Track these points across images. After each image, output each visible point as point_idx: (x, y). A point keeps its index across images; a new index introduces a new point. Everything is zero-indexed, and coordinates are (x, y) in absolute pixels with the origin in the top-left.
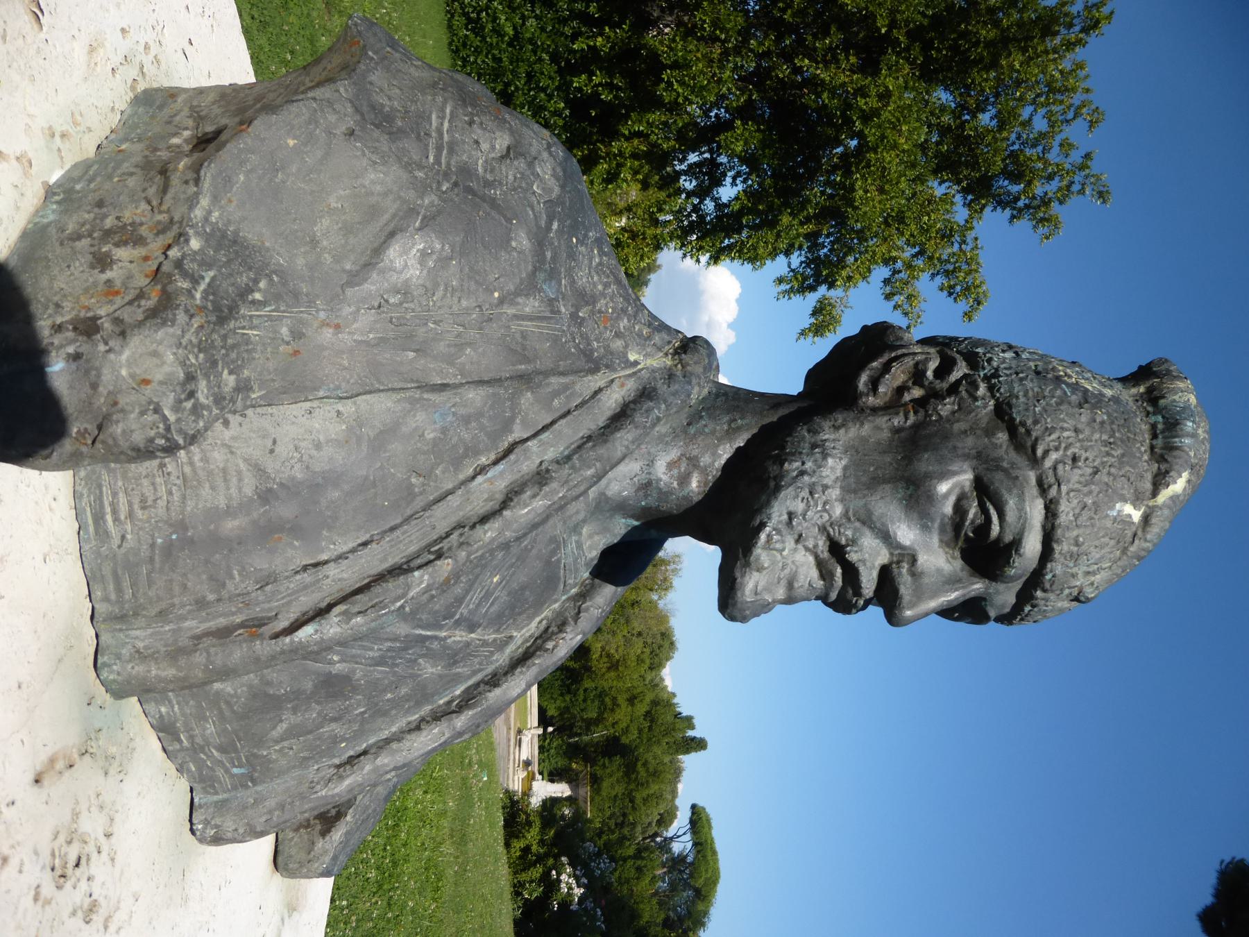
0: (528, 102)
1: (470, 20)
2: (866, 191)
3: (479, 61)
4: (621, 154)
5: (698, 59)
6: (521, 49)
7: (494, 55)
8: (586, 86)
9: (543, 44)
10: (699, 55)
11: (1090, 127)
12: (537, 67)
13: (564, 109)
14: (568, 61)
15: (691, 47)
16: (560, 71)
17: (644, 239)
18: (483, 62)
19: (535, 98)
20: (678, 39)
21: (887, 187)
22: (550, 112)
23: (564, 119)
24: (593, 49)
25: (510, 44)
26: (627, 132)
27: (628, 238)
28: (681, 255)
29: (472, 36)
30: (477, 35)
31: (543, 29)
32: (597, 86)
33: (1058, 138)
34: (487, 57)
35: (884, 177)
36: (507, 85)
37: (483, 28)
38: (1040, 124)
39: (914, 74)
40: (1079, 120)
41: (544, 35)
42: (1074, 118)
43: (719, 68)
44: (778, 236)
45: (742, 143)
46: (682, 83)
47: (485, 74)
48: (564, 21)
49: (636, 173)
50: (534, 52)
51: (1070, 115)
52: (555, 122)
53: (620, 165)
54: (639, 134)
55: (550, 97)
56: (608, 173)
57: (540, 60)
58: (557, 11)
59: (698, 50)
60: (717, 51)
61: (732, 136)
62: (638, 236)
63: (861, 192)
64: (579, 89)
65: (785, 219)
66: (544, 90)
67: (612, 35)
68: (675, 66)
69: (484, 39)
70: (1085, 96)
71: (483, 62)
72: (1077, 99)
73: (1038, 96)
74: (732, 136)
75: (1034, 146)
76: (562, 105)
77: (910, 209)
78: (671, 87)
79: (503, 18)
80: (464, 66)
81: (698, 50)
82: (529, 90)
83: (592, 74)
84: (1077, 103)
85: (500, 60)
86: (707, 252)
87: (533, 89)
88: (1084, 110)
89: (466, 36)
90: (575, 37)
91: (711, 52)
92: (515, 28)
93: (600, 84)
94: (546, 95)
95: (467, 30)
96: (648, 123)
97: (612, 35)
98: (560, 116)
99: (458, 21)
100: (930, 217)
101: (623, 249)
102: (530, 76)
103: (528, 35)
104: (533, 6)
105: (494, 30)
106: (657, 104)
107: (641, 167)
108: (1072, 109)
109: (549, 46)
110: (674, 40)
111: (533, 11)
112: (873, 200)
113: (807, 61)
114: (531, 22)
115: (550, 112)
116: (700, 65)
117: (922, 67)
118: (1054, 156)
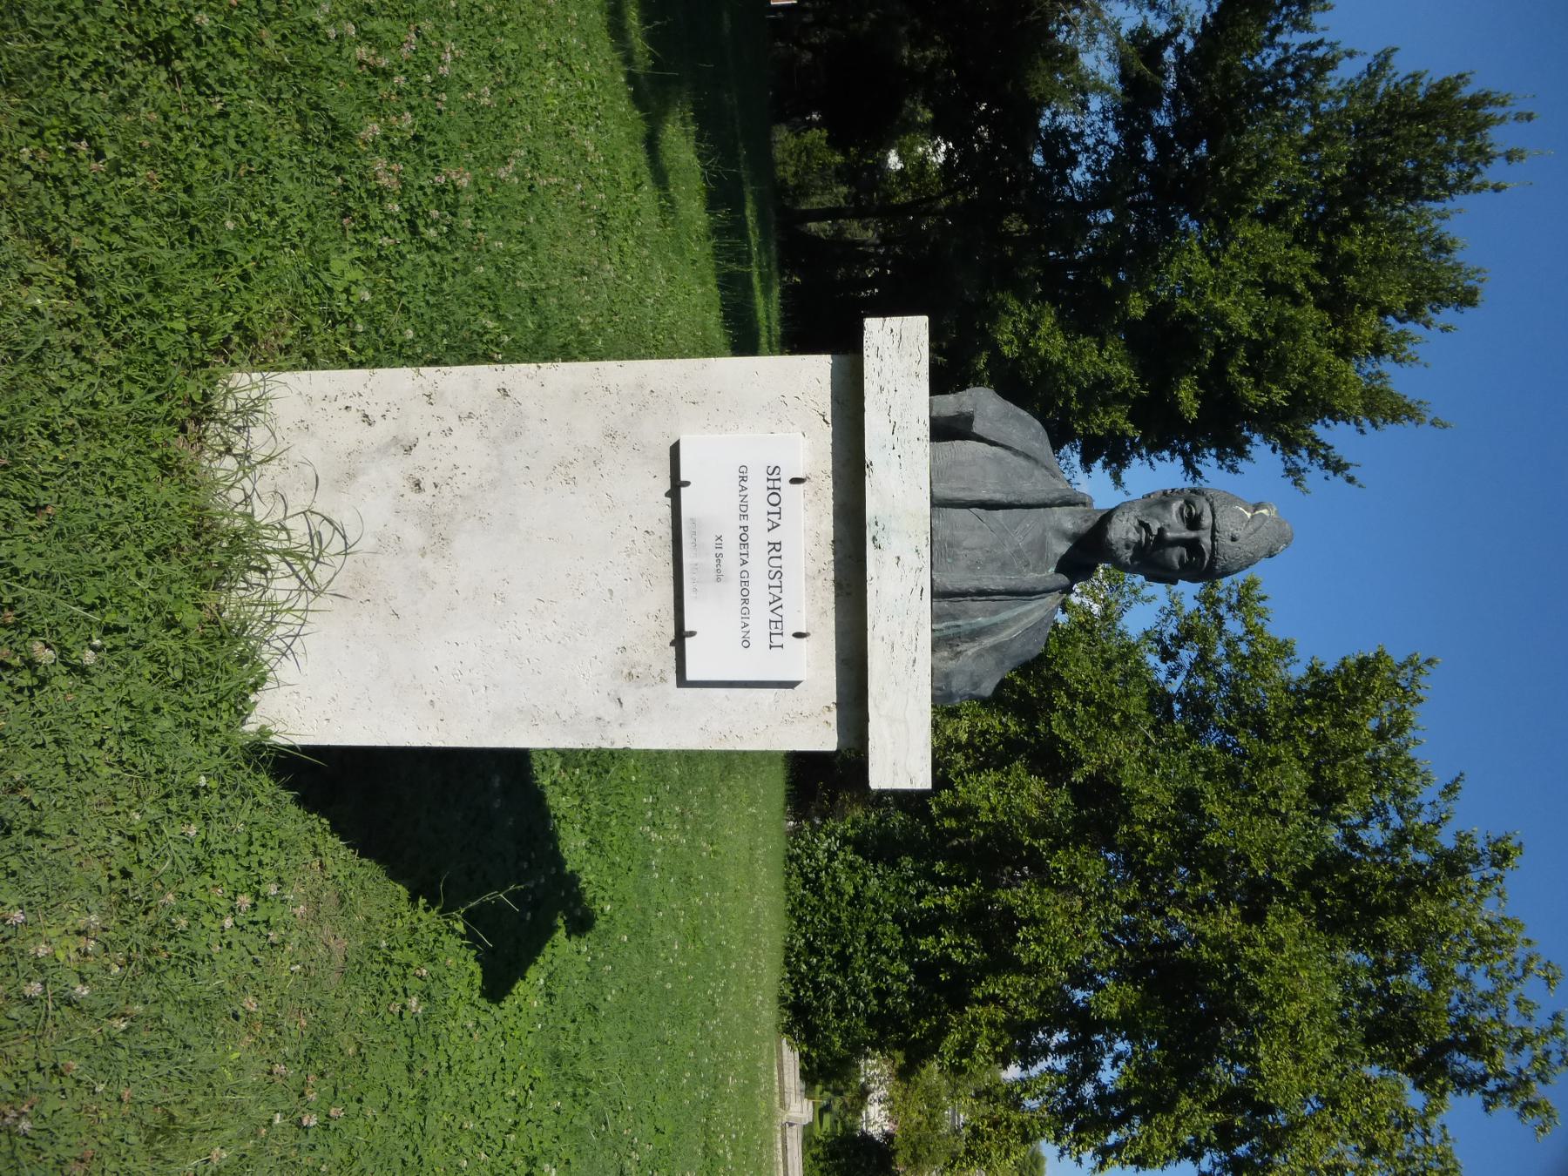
0: (869, 966)
1: (807, 880)
2: (1275, 1058)
3: (816, 921)
4: (975, 1021)
5: (1056, 913)
6: (862, 908)
7: (832, 914)
8: (934, 948)
9: (885, 903)
10: (1057, 909)
11: (1549, 984)
12: (879, 928)
13: (908, 973)
14: (913, 922)
15: (1048, 900)
16: (904, 933)
17: (1008, 1127)
18: (820, 921)
19: (876, 960)
20: (1033, 890)
21: (1303, 1053)
22: (892, 975)
23: (908, 984)
24: (941, 908)
25: (850, 903)
26: (980, 995)
27: (988, 1126)
28: (1058, 1154)
29: (809, 895)
30: (815, 894)
31: (885, 889)
32: (946, 948)
33: (1511, 996)
34: (824, 916)
35: (1297, 1043)
36: (845, 946)
37: (822, 887)
38: (1482, 983)
39: (1310, 925)
40: (1530, 976)
41: (887, 894)
42: (1524, 975)
43: (1081, 923)
44: (1178, 1124)
45: (1117, 1003)
46: (1039, 941)
47: (822, 935)
48: (908, 881)
49: (994, 1044)
50: (876, 911)
51: (1519, 973)
52: (898, 989)
53: (974, 1036)
54: (994, 998)
55: (893, 960)
56: (961, 1043)
57: (883, 921)
58: (901, 871)
59: (1057, 904)
60: (1078, 904)
61: (1104, 997)
62: (1001, 1123)
63: (1267, 1059)
64: (926, 953)
65: (1185, 1103)
66: (885, 952)
67: (961, 893)
68: (1033, 921)
69: (822, 898)
70: (1528, 950)
71: (820, 921)
72: (1520, 952)
73: (1471, 950)
74: (1104, 997)
75: (1483, 1007)
76: (906, 968)
77: (1343, 1089)
78: (1028, 951)
79: (843, 877)
80: (799, 926)
81: (1057, 904)
82: (870, 952)
83: (939, 935)
84: (1522, 958)
85: (839, 919)
86: (1090, 1145)
87: (874, 951)
88: (1533, 966)
89: (803, 895)
90: (921, 895)
91: (1072, 906)
92: (855, 888)
93: (950, 945)
94: (888, 957)
95: (804, 888)
96: (1004, 984)
97: (961, 893)
98: (904, 981)
99: (796, 881)
100: (1372, 1098)
101: (983, 1141)
102: (871, 937)
103: (869, 894)
104: (875, 866)
105: (833, 889)
106: (1016, 967)
107: (1002, 1038)
108: (1518, 964)
109: (892, 905)
110: (1029, 892)
111: (875, 871)
112: (1286, 1069)
113: (1180, 912)
114: (874, 882)
115: (892, 975)
116: (1060, 920)
117: (1320, 914)
118: (1512, 1019)
